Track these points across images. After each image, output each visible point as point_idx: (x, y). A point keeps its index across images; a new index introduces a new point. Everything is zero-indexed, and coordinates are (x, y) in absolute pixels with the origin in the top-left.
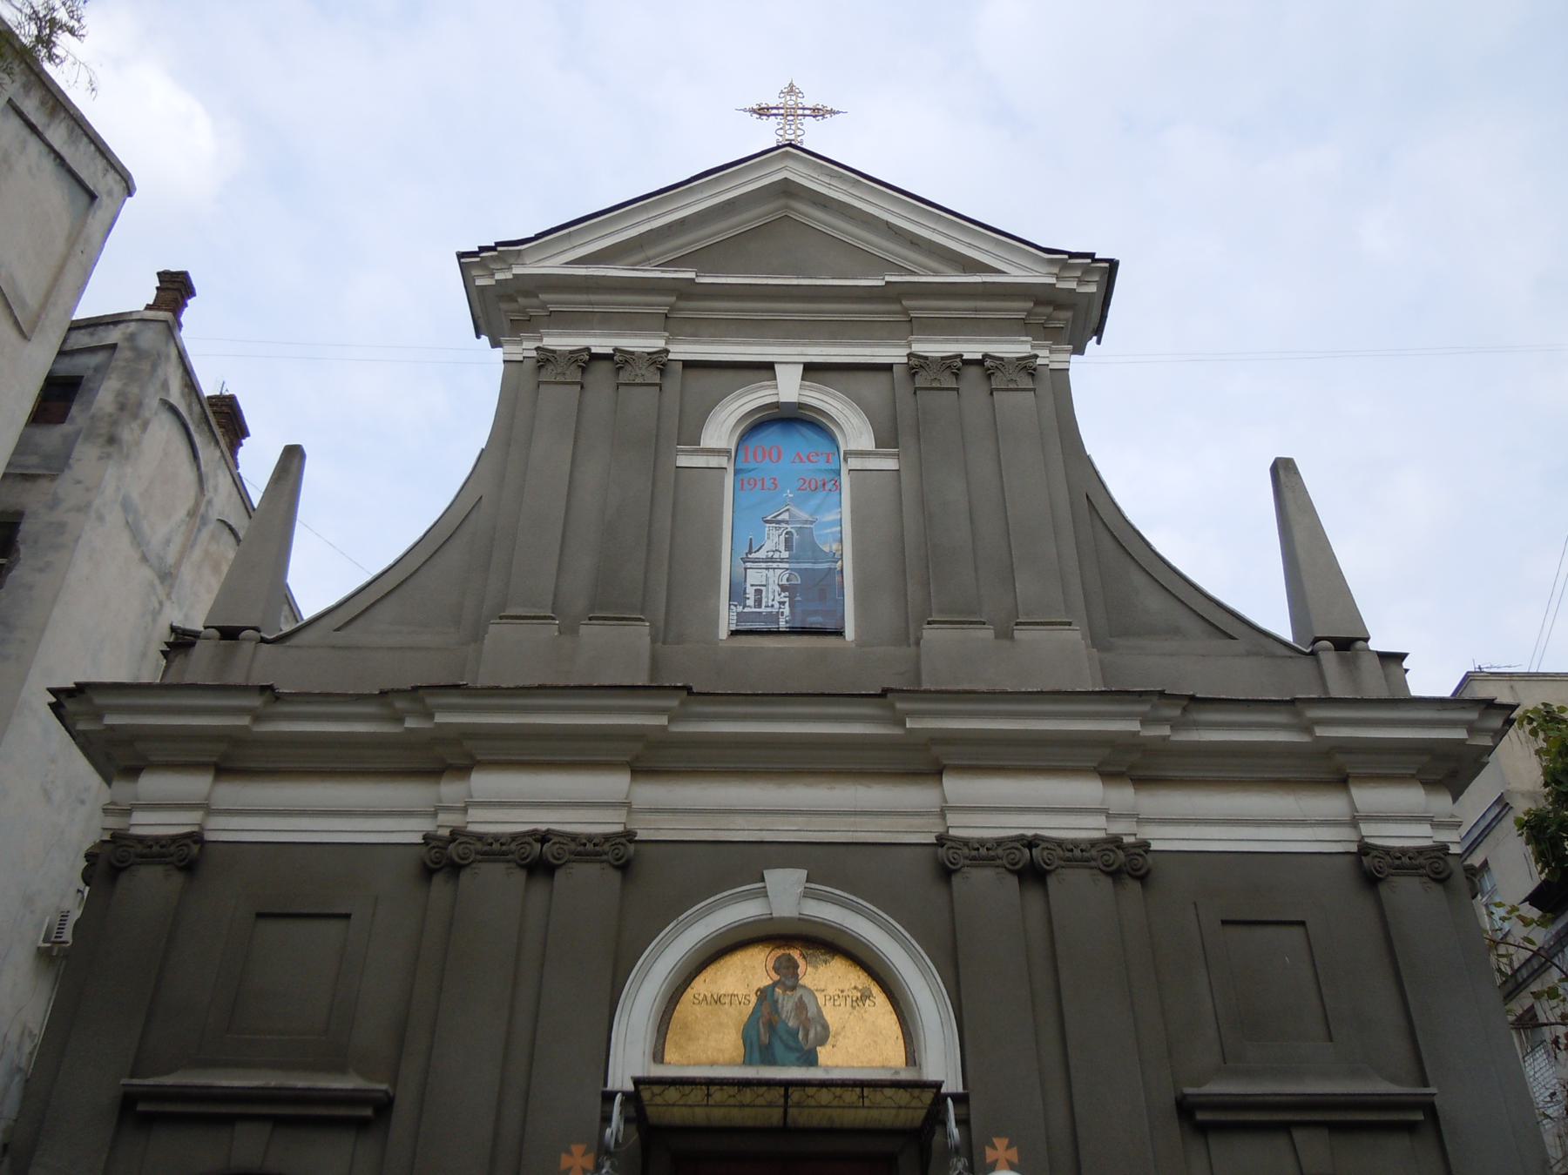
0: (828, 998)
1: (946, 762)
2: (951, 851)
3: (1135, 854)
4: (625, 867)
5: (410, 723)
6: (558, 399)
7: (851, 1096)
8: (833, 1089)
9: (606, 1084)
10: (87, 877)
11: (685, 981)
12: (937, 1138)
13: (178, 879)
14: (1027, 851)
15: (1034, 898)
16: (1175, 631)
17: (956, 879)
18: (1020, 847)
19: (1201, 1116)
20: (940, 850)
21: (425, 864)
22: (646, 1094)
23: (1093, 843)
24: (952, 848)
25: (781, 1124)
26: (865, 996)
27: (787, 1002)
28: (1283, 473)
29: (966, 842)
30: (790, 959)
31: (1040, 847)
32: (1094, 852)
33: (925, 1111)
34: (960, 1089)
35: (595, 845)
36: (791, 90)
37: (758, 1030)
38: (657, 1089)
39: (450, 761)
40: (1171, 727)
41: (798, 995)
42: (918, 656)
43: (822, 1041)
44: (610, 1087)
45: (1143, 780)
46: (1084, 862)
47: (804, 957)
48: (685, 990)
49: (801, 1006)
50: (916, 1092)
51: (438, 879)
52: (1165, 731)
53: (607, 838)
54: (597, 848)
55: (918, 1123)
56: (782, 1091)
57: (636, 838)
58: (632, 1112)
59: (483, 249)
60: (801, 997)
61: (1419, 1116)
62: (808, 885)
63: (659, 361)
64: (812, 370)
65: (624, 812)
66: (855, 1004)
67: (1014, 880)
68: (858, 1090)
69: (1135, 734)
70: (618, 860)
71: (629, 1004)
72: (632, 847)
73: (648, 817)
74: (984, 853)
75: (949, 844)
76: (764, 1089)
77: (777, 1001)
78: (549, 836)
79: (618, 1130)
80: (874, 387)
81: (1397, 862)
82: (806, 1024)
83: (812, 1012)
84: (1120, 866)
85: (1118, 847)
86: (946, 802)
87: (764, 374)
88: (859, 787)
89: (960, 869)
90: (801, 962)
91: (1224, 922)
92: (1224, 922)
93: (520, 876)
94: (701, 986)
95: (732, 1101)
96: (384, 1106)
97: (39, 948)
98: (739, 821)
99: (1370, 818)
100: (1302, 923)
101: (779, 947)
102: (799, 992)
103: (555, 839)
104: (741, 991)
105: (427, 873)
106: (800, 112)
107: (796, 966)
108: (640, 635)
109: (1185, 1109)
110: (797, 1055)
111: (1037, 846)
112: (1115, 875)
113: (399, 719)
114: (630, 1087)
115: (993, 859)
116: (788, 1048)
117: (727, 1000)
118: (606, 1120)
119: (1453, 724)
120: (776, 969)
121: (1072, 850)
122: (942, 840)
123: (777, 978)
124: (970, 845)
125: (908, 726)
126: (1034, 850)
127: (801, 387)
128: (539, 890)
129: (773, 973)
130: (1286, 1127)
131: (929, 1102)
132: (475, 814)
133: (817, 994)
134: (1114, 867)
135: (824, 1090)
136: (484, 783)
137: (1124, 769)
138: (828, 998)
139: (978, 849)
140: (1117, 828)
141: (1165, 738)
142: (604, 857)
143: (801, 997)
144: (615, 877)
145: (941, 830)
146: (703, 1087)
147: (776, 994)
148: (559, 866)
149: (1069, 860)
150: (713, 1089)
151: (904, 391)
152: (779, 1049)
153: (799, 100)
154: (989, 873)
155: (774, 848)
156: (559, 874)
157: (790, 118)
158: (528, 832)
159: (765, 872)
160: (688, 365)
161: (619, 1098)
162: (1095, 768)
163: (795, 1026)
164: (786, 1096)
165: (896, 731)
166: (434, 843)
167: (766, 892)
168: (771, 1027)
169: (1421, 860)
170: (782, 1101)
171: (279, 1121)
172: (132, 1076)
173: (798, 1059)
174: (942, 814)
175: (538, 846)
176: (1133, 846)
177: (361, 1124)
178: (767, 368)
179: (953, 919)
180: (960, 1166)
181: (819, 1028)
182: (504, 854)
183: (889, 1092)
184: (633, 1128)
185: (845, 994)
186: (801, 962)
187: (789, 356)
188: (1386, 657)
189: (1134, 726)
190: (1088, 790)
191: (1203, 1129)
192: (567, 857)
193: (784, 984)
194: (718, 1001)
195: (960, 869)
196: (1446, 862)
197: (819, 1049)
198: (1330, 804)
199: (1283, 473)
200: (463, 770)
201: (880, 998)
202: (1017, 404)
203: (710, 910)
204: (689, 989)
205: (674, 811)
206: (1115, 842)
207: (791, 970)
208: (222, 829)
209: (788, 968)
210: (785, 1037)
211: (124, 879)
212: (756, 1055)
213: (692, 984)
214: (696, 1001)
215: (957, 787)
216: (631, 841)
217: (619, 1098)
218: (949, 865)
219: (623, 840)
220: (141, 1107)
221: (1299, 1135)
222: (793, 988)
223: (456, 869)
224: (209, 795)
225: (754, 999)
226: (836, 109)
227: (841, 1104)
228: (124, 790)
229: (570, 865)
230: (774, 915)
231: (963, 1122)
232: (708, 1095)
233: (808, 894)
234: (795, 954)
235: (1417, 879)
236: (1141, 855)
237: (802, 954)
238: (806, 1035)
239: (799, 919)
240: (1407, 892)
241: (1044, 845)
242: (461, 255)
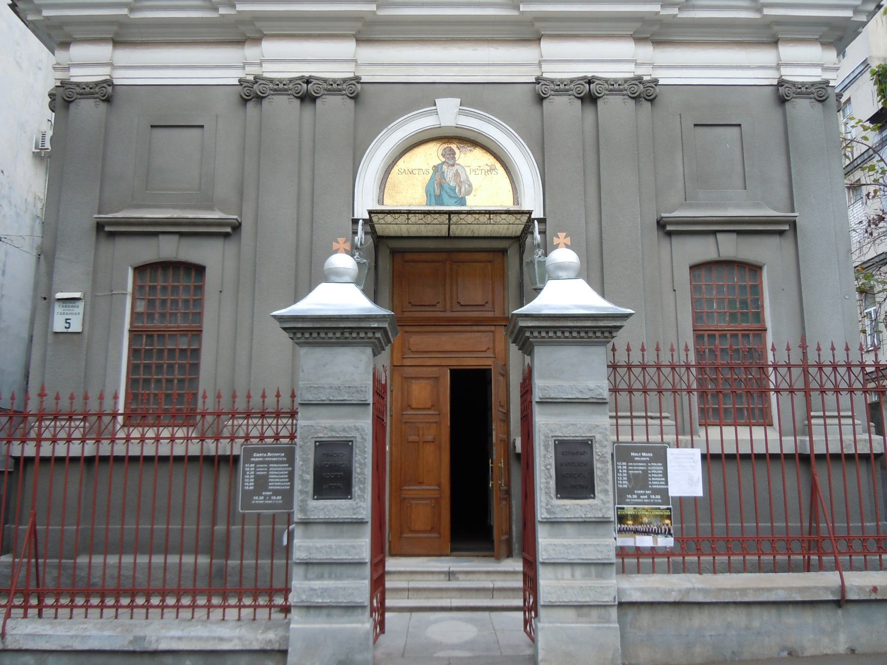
0: (472, 170)
1: (542, 33)
2: (544, 86)
3: (650, 87)
4: (355, 98)
5: (223, 11)
7: (484, 218)
8: (474, 215)
9: (353, 215)
11: (393, 162)
12: (528, 240)
13: (103, 106)
14: (587, 85)
15: (589, 111)
17: (545, 103)
18: (583, 83)
19: (669, 228)
20: (537, 85)
21: (241, 96)
22: (375, 218)
23: (626, 81)
24: (545, 85)
25: (447, 235)
26: (492, 169)
27: (449, 173)
29: (552, 81)
30: (451, 149)
31: (595, 83)
32: (626, 86)
33: (523, 226)
34: (542, 216)
35: (338, 85)
37: (434, 188)
38: (381, 216)
39: (248, 35)
40: (679, 9)
41: (456, 169)
43: (469, 193)
44: (356, 217)
45: (658, 42)
47: (459, 149)
48: (393, 166)
49: (457, 174)
50: (519, 216)
51: (250, 105)
52: (674, 11)
53: (345, 81)
54: (339, 87)
55: (519, 233)
56: (447, 216)
57: (361, 81)
58: (368, 229)
60: (457, 170)
61: (786, 227)
62: (461, 108)
65: (353, 65)
66: (486, 173)
68: (487, 216)
69: (657, 13)
70: (352, 93)
71: (363, 173)
72: (359, 86)
73: (368, 68)
74: (562, 88)
75: (543, 82)
76: (438, 215)
77: (444, 173)
78: (311, 80)
79: (362, 238)
81: (799, 90)
82: (460, 184)
83: (463, 178)
84: (640, 94)
85: (640, 83)
86: (542, 57)
88: (491, 49)
89: (548, 97)
90: (457, 151)
91: (695, 125)
92: (695, 125)
93: (298, 102)
94: (401, 164)
95: (421, 222)
96: (237, 227)
97: (33, 152)
98: (421, 70)
99: (787, 65)
100: (740, 125)
101: (445, 143)
102: (456, 167)
103: (315, 81)
104: (424, 167)
105: (245, 101)
107: (454, 154)
109: (661, 224)
110: (456, 200)
111: (593, 82)
112: (636, 98)
114: (367, 216)
115: (567, 90)
116: (449, 196)
117: (417, 172)
118: (355, 233)
120: (443, 155)
121: (613, 85)
122: (538, 80)
123: (444, 160)
124: (555, 82)
125: (521, 10)
126: (591, 85)
128: (308, 109)
129: (441, 157)
130: (714, 233)
131: (525, 221)
132: (267, 67)
133: (466, 168)
134: (636, 95)
135: (470, 216)
136: (270, 48)
137: (649, 36)
138: (472, 170)
139: (559, 85)
140: (640, 71)
141: (675, 16)
142: (344, 92)
143: (457, 170)
144: (351, 103)
145: (539, 74)
146: (406, 215)
147: (443, 169)
148: (318, 97)
149: (611, 90)
150: (410, 216)
152: (445, 197)
155: (442, 85)
156: (318, 101)
158: (299, 77)
159: (436, 100)
161: (361, 222)
162: (631, 35)
163: (454, 185)
164: (450, 219)
165: (514, 13)
166: (245, 84)
167: (437, 112)
168: (441, 186)
169: (813, 89)
170: (447, 222)
171: (181, 234)
172: (99, 213)
173: (456, 202)
174: (540, 64)
175: (305, 85)
176: (649, 82)
177: (226, 235)
179: (543, 125)
180: (540, 253)
181: (467, 186)
182: (286, 90)
183: (503, 216)
184: (369, 237)
185: (481, 168)
186: (457, 151)
189: (656, 8)
190: (626, 48)
191: (670, 234)
192: (322, 92)
193: (447, 163)
194: (412, 172)
195: (548, 97)
196: (827, 91)
197: (466, 197)
198: (765, 56)
200: (257, 40)
203: (406, 122)
204: (395, 166)
205: (382, 65)
206: (639, 79)
207: (452, 155)
208: (122, 78)
209: (450, 154)
210: (449, 191)
211: (72, 106)
212: (433, 200)
213: (397, 163)
214: (400, 173)
215: (549, 48)
216: (358, 83)
217: (361, 222)
218: (542, 95)
219: (354, 82)
220: (107, 229)
221: (720, 237)
222: (453, 165)
223: (259, 99)
224: (112, 57)
225: (431, 172)
227: (479, 223)
228: (62, 56)
229: (324, 97)
230: (442, 125)
231: (542, 232)
232: (408, 219)
233: (461, 113)
234: (454, 146)
235: (808, 100)
236: (653, 87)
237: (457, 147)
238: (460, 190)
239: (456, 127)
240: (802, 108)
241: (597, 82)
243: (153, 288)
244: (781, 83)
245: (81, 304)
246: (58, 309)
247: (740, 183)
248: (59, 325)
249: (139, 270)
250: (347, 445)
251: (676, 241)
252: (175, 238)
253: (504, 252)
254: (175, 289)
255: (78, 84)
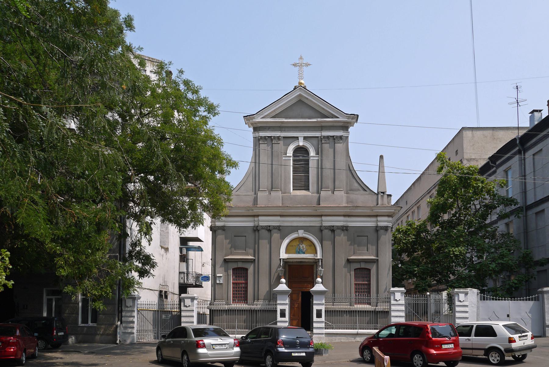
4: (279, 230)
6: (263, 146)
10: (211, 230)
16: (359, 190)
27: (301, 246)
28: (381, 157)
36: (301, 58)
42: (319, 197)
46: (340, 229)
49: (303, 246)
59: (247, 116)
63: (278, 138)
64: (305, 138)
67: (330, 232)
80: (315, 141)
87: (297, 139)
94: (290, 244)
99: (379, 222)
106: (303, 65)
108: (280, 194)
112: (343, 230)
113: (249, 210)
119: (392, 209)
127: (303, 141)
136: (261, 218)
151: (320, 143)
152: (300, 252)
153: (303, 61)
154: (327, 230)
157: (301, 67)
160: (284, 137)
177: (252, 262)
178: (297, 138)
187: (301, 135)
188: (388, 195)
190: (342, 218)
191: (350, 262)
199: (381, 157)
201: (313, 245)
202: (339, 146)
211: (217, 231)
226: (310, 64)
240: (382, 232)
242: (244, 117)
243: (236, 273)
244: (377, 227)
245: (222, 278)
246: (217, 278)
247: (366, 250)
248: (218, 282)
249: (233, 269)
250: (285, 310)
251: (352, 264)
252: (241, 262)
253: (313, 265)
254: (241, 273)
255: (218, 226)
